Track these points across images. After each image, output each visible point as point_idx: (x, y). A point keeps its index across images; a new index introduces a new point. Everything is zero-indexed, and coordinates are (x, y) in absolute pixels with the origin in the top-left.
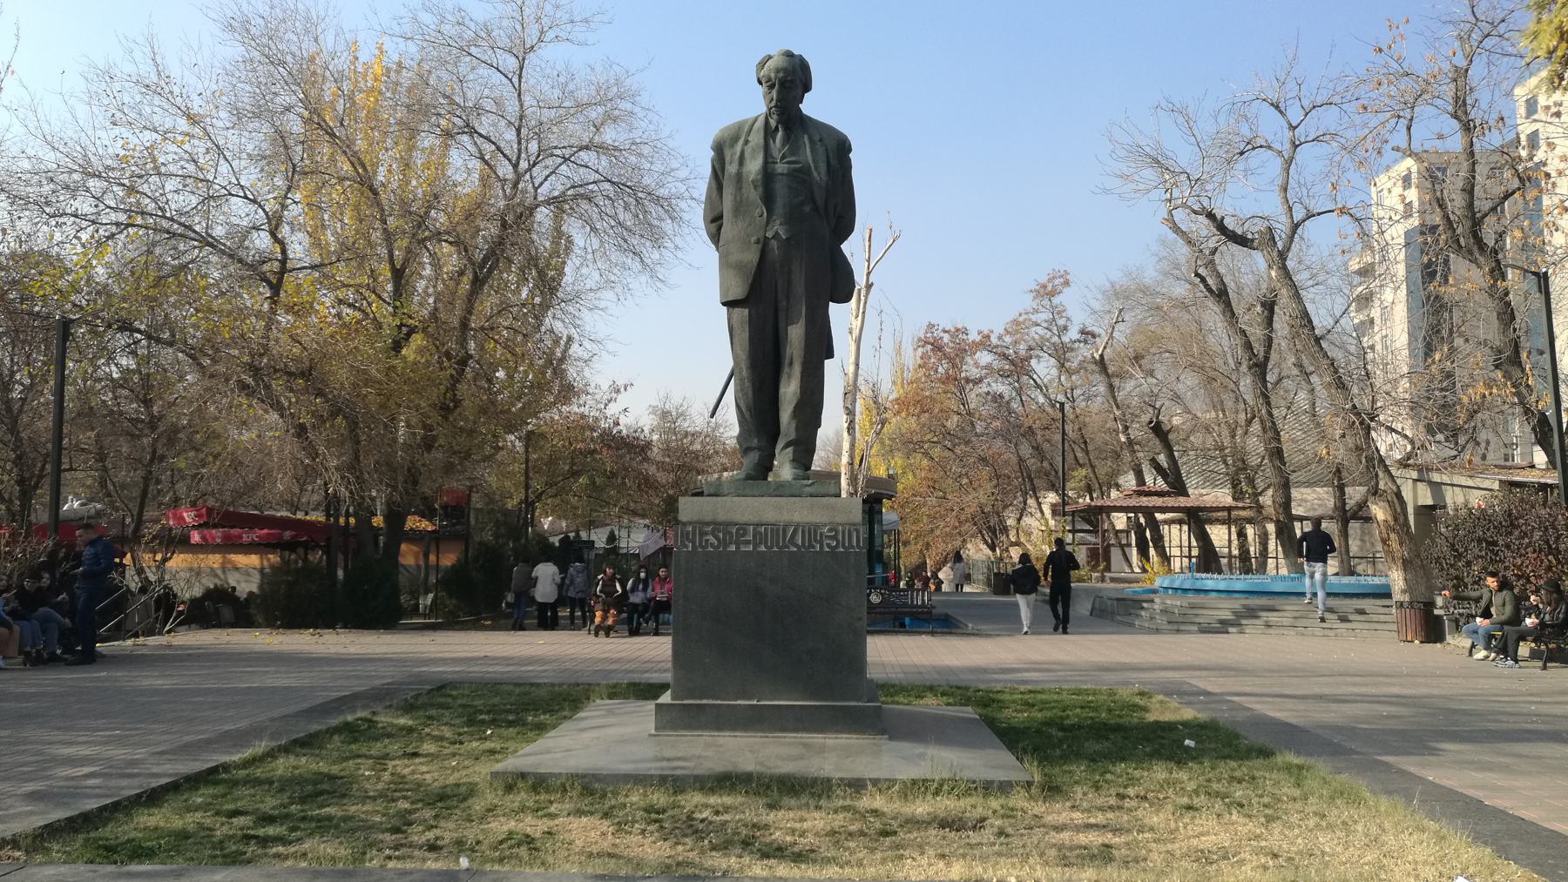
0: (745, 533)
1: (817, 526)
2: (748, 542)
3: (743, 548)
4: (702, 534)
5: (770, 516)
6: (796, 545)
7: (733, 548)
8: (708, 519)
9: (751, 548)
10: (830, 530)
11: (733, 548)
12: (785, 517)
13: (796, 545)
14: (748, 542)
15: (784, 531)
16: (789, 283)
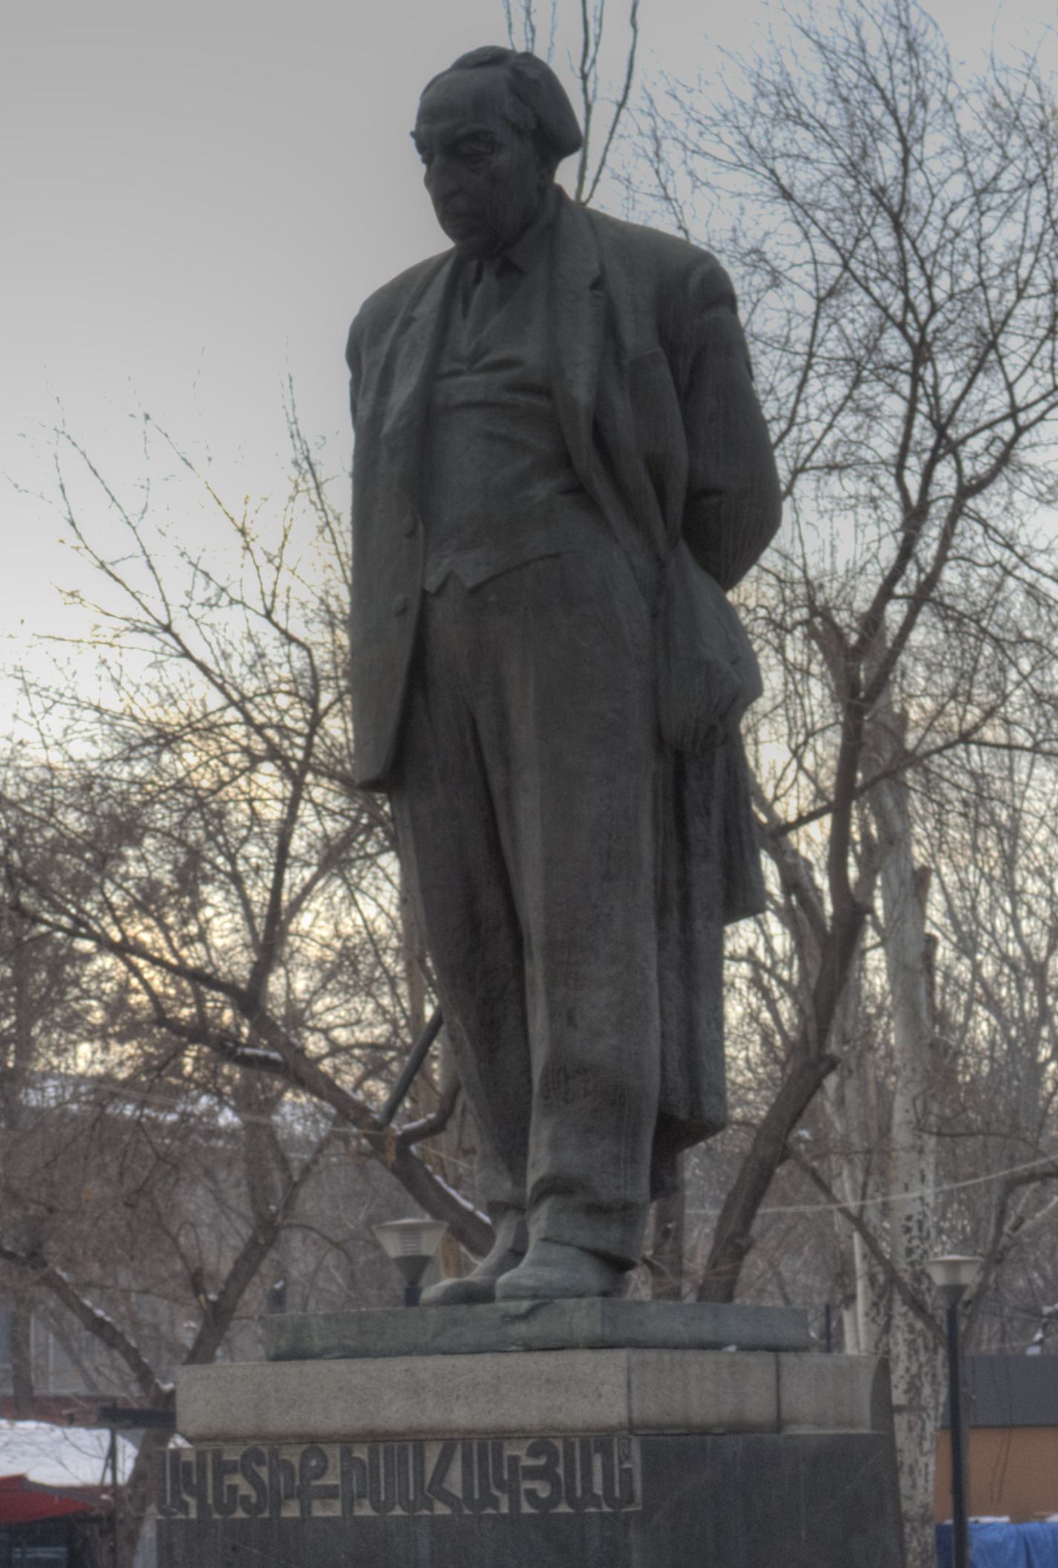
0: (322, 1472)
1: (502, 1436)
2: (329, 1493)
3: (318, 1511)
4: (223, 1469)
5: (395, 1413)
6: (447, 1498)
7: (291, 1511)
8: (245, 1425)
9: (335, 1510)
10: (533, 1453)
11: (291, 1511)
12: (431, 1414)
13: (447, 1498)
14: (329, 1493)
15: (420, 1458)
16: (503, 716)
